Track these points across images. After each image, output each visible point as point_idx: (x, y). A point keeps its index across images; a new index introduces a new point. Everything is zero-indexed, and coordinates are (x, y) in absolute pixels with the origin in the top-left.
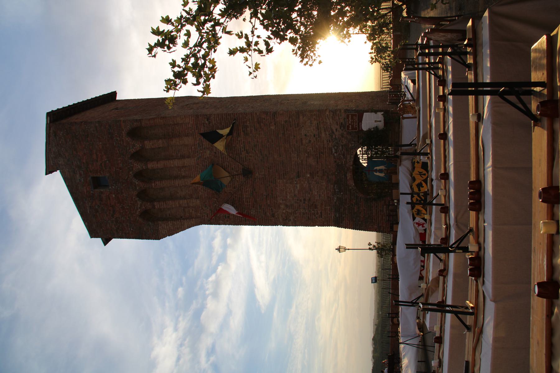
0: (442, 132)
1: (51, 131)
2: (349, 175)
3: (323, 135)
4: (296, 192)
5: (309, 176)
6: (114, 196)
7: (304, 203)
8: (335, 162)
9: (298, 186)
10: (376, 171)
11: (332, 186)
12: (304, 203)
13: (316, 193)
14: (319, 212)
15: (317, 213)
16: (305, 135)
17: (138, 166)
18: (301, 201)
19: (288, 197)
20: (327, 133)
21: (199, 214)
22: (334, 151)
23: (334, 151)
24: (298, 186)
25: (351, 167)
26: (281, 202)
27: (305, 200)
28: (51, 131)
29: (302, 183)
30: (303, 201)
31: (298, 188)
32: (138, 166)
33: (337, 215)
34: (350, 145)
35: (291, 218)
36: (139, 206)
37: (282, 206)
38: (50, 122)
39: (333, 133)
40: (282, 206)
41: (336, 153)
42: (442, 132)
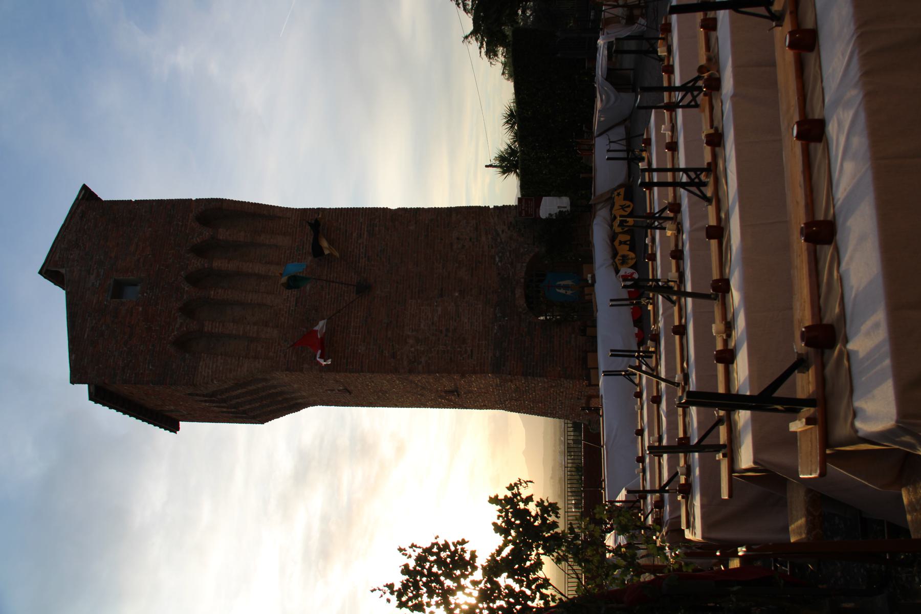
0: (655, 394)
1: (79, 211)
2: (519, 292)
3: (484, 239)
6: (141, 309)
7: (446, 336)
8: (499, 274)
9: (440, 309)
10: (560, 287)
13: (466, 320)
16: (458, 239)
18: (441, 332)
19: (422, 326)
20: (490, 237)
21: (271, 354)
22: (497, 259)
23: (497, 259)
25: (522, 280)
26: (409, 333)
27: (447, 330)
28: (79, 211)
31: (439, 313)
33: (498, 354)
34: (522, 250)
35: (423, 360)
36: (178, 326)
37: (411, 341)
38: (83, 198)
39: (498, 235)
40: (411, 341)
41: (501, 261)
42: (655, 394)
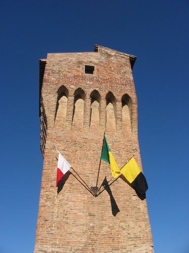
4: (74, 211)
5: (91, 225)
9: (81, 214)
11: (80, 248)
12: (64, 218)
13: (73, 231)
14: (53, 232)
15: (52, 230)
17: (103, 94)
18: (66, 215)
19: (70, 203)
24: (81, 214)
26: (66, 196)
29: (85, 218)
30: (66, 216)
31: (79, 214)
32: (103, 94)
35: (48, 204)
36: (72, 86)
